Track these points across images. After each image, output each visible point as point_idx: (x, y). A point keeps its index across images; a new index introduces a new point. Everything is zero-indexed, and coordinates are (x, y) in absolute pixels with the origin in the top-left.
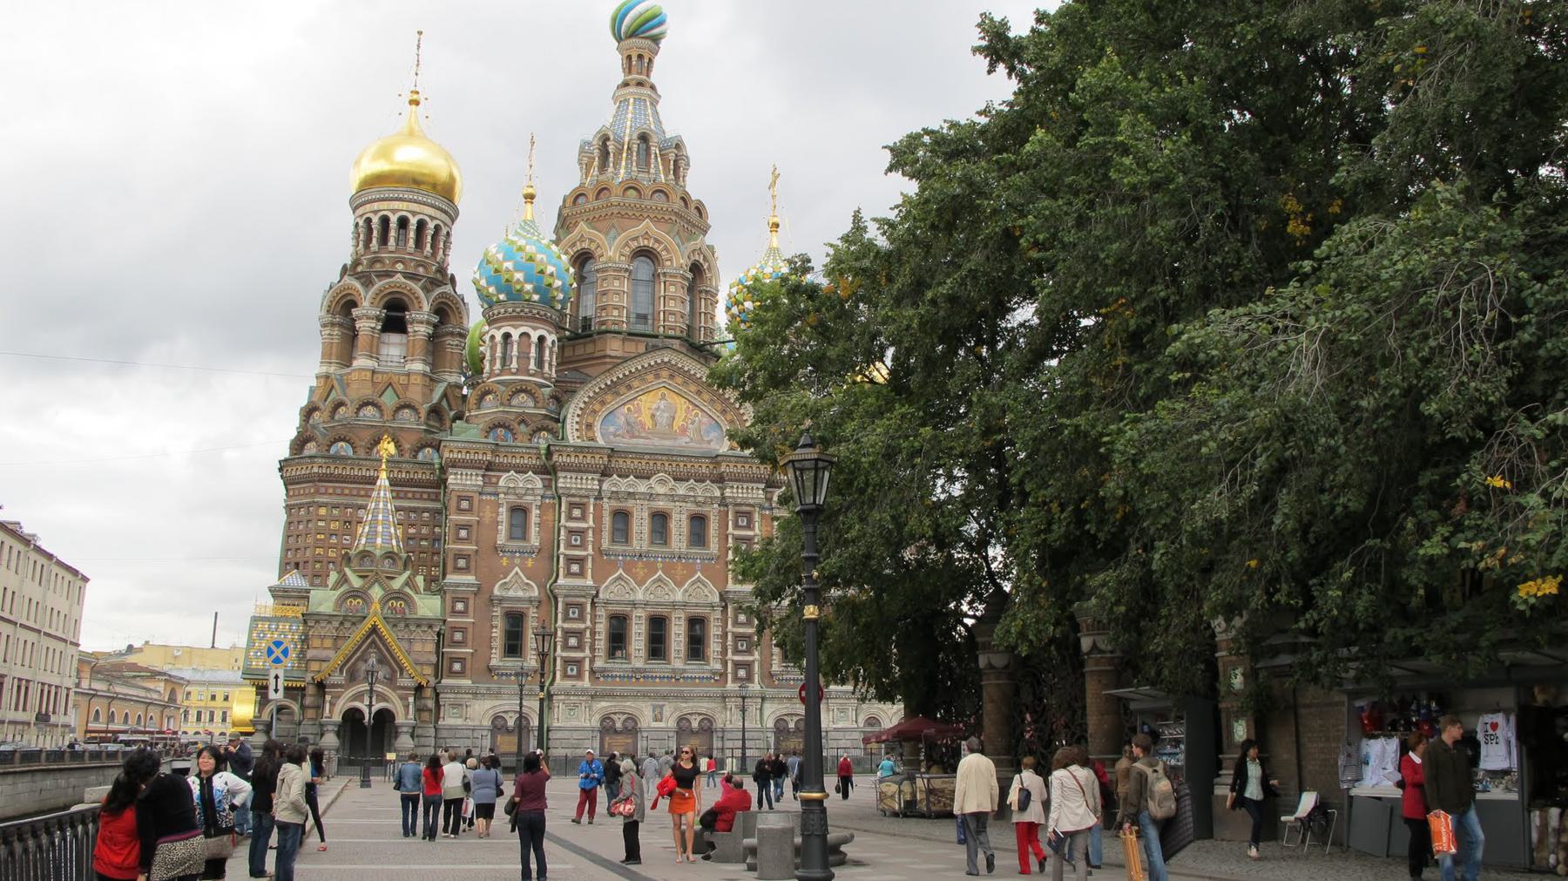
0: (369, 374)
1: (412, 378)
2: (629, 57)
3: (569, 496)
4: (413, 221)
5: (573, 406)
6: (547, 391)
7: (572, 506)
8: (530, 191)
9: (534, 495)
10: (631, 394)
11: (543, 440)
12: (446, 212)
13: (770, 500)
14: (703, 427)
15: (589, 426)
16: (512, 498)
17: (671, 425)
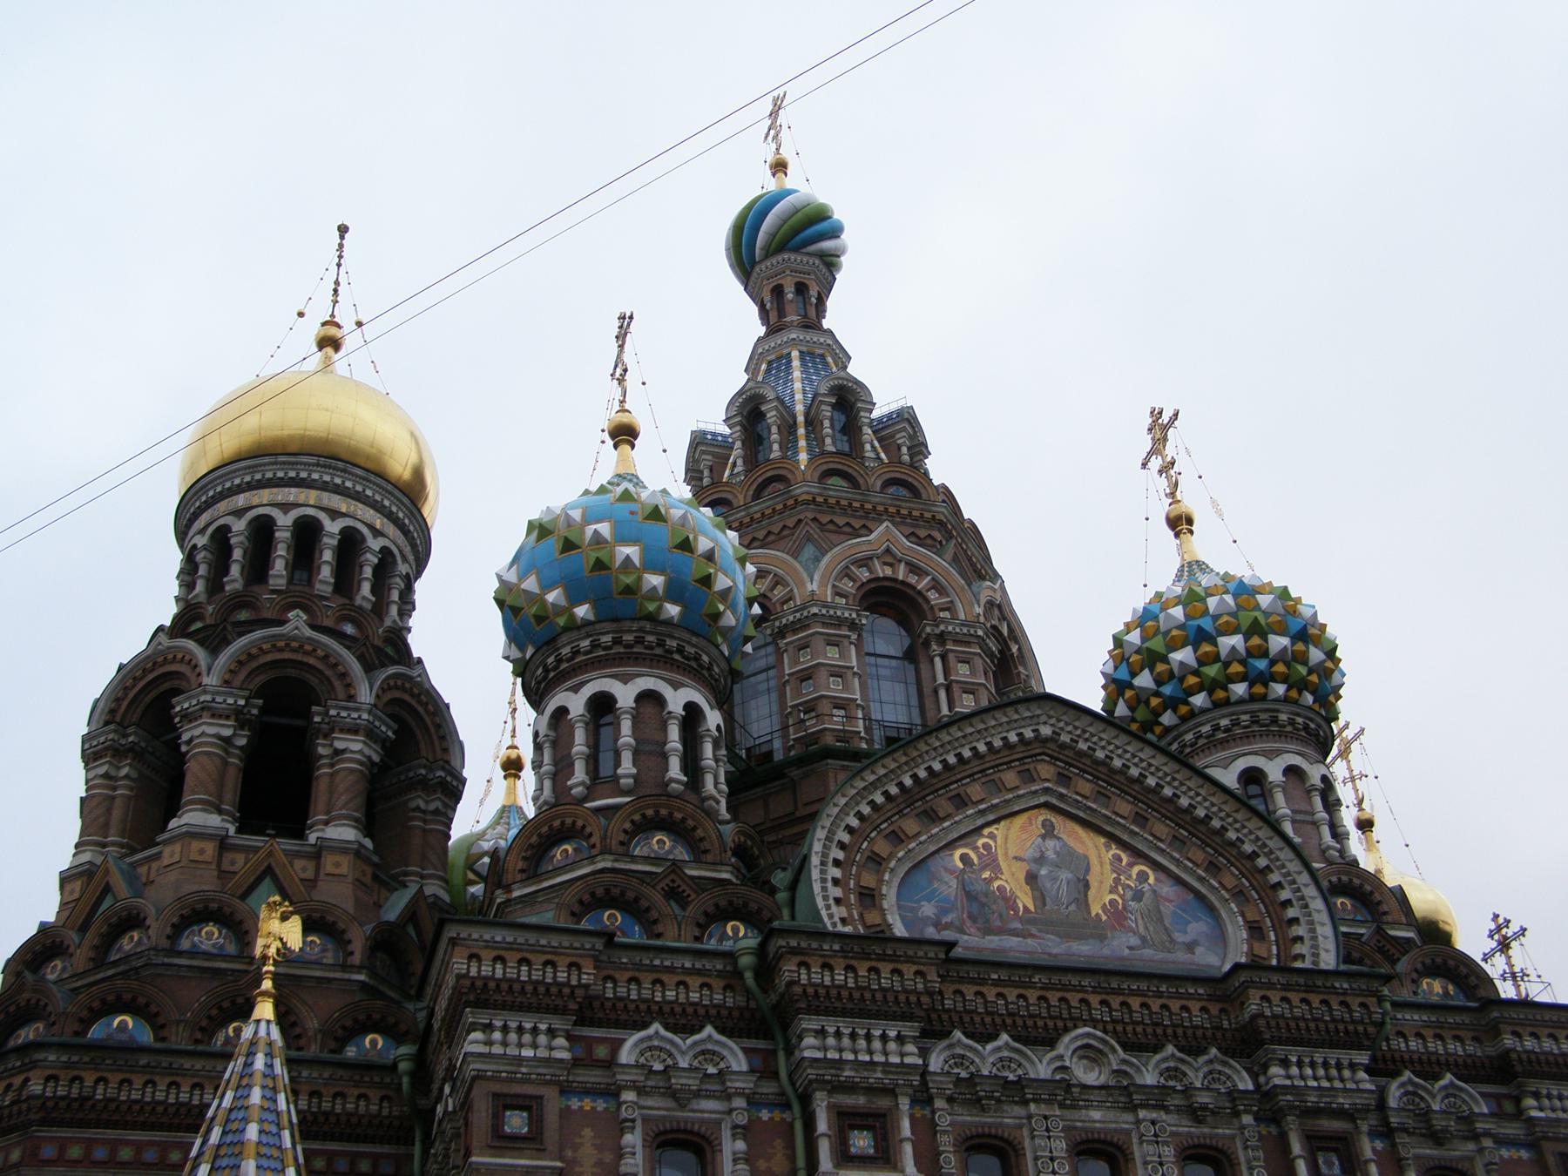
0: (210, 848)
1: (329, 863)
2: (778, 291)
3: (836, 1087)
4: (333, 527)
5: (821, 834)
6: (728, 830)
7: (847, 1120)
8: (624, 418)
9: (727, 1096)
10: (965, 819)
11: (739, 936)
12: (406, 532)
13: (1382, 1105)
14: (1167, 909)
15: (869, 897)
16: (658, 1106)
17: (1082, 901)
